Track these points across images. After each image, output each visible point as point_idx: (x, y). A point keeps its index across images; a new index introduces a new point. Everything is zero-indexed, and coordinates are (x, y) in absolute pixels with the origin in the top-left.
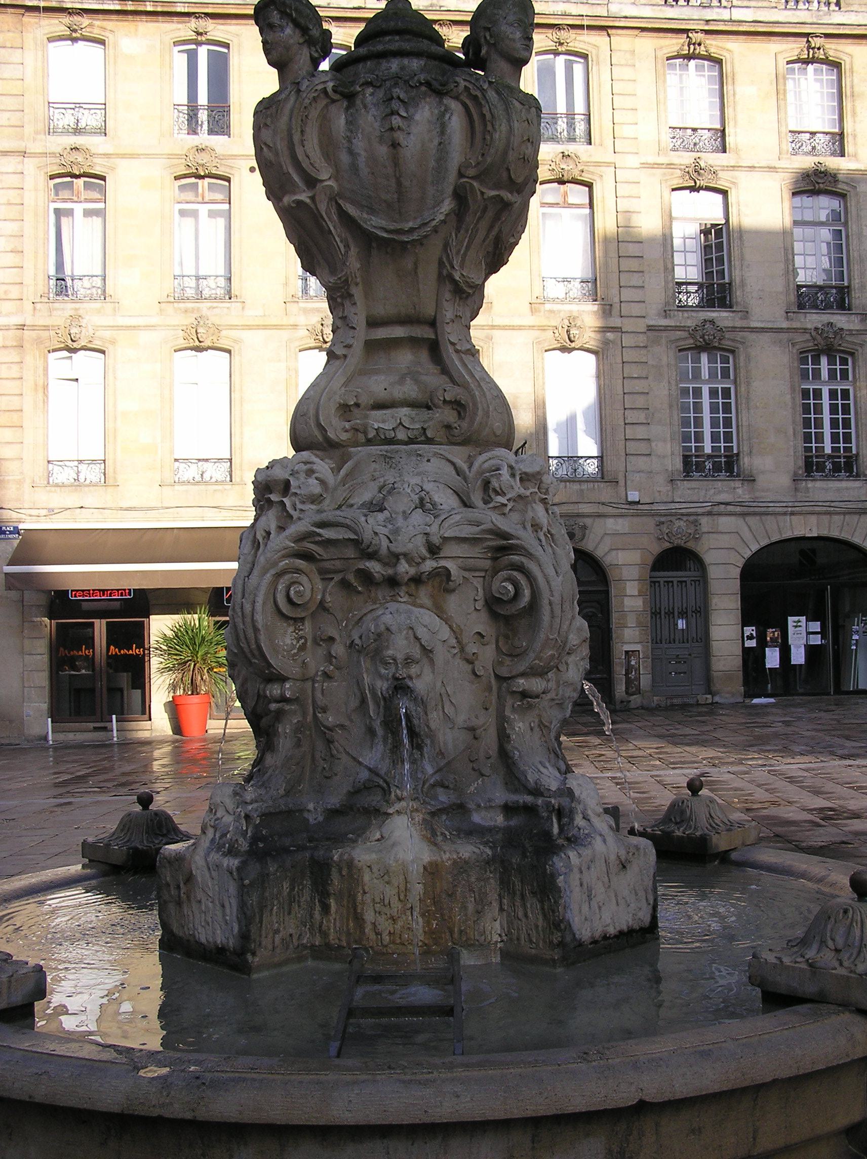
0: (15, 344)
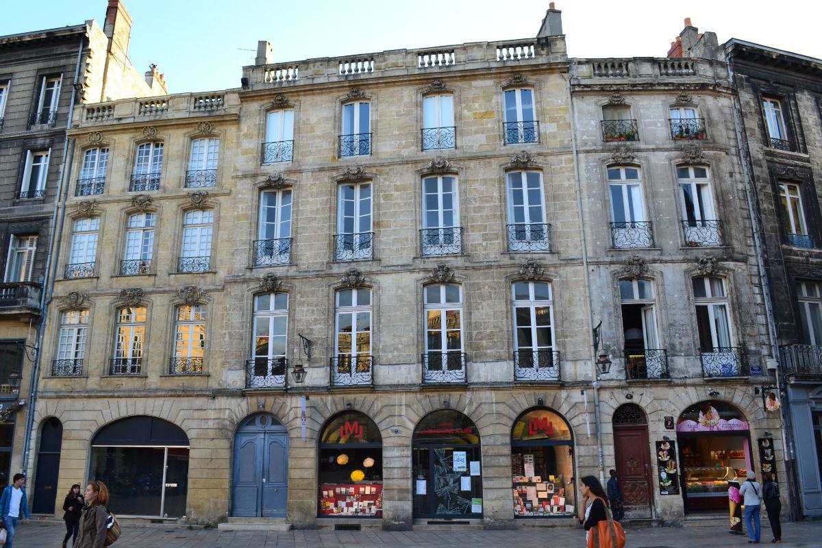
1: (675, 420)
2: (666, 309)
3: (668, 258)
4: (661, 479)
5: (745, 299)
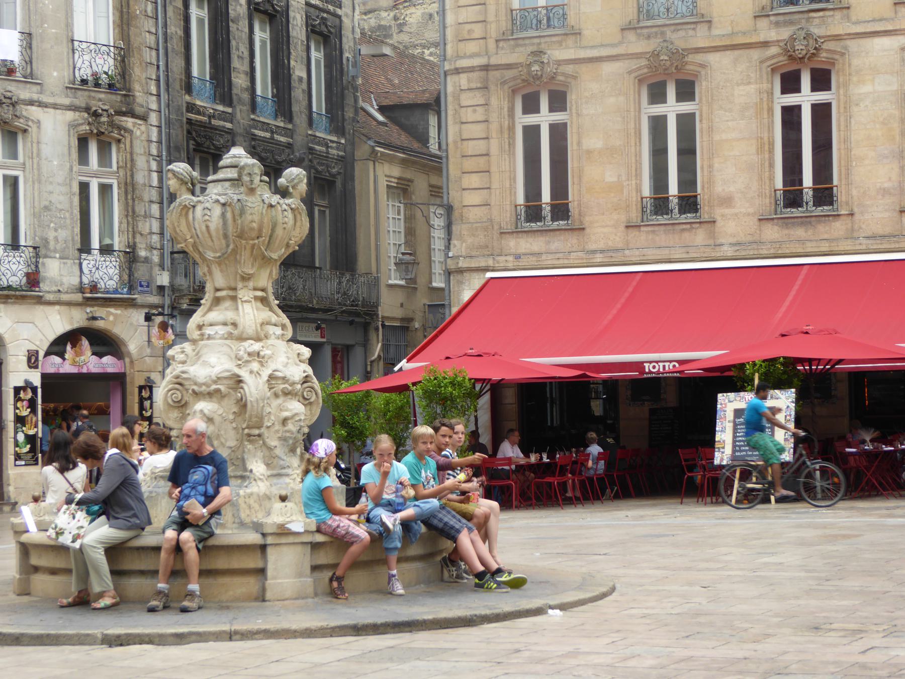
0: (479, 85)
1: (41, 354)
2: (40, 182)
3: (51, 100)
4: (16, 444)
5: (140, 178)
